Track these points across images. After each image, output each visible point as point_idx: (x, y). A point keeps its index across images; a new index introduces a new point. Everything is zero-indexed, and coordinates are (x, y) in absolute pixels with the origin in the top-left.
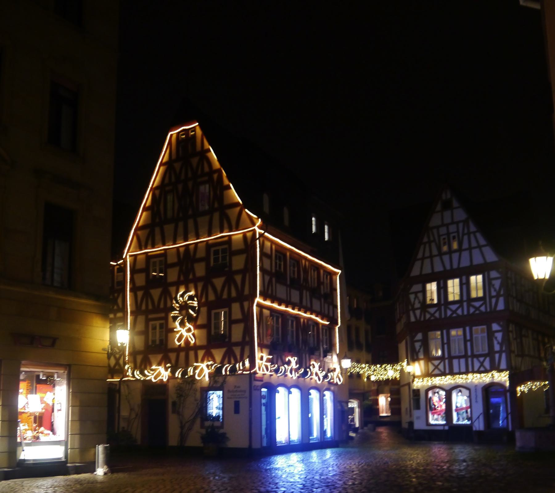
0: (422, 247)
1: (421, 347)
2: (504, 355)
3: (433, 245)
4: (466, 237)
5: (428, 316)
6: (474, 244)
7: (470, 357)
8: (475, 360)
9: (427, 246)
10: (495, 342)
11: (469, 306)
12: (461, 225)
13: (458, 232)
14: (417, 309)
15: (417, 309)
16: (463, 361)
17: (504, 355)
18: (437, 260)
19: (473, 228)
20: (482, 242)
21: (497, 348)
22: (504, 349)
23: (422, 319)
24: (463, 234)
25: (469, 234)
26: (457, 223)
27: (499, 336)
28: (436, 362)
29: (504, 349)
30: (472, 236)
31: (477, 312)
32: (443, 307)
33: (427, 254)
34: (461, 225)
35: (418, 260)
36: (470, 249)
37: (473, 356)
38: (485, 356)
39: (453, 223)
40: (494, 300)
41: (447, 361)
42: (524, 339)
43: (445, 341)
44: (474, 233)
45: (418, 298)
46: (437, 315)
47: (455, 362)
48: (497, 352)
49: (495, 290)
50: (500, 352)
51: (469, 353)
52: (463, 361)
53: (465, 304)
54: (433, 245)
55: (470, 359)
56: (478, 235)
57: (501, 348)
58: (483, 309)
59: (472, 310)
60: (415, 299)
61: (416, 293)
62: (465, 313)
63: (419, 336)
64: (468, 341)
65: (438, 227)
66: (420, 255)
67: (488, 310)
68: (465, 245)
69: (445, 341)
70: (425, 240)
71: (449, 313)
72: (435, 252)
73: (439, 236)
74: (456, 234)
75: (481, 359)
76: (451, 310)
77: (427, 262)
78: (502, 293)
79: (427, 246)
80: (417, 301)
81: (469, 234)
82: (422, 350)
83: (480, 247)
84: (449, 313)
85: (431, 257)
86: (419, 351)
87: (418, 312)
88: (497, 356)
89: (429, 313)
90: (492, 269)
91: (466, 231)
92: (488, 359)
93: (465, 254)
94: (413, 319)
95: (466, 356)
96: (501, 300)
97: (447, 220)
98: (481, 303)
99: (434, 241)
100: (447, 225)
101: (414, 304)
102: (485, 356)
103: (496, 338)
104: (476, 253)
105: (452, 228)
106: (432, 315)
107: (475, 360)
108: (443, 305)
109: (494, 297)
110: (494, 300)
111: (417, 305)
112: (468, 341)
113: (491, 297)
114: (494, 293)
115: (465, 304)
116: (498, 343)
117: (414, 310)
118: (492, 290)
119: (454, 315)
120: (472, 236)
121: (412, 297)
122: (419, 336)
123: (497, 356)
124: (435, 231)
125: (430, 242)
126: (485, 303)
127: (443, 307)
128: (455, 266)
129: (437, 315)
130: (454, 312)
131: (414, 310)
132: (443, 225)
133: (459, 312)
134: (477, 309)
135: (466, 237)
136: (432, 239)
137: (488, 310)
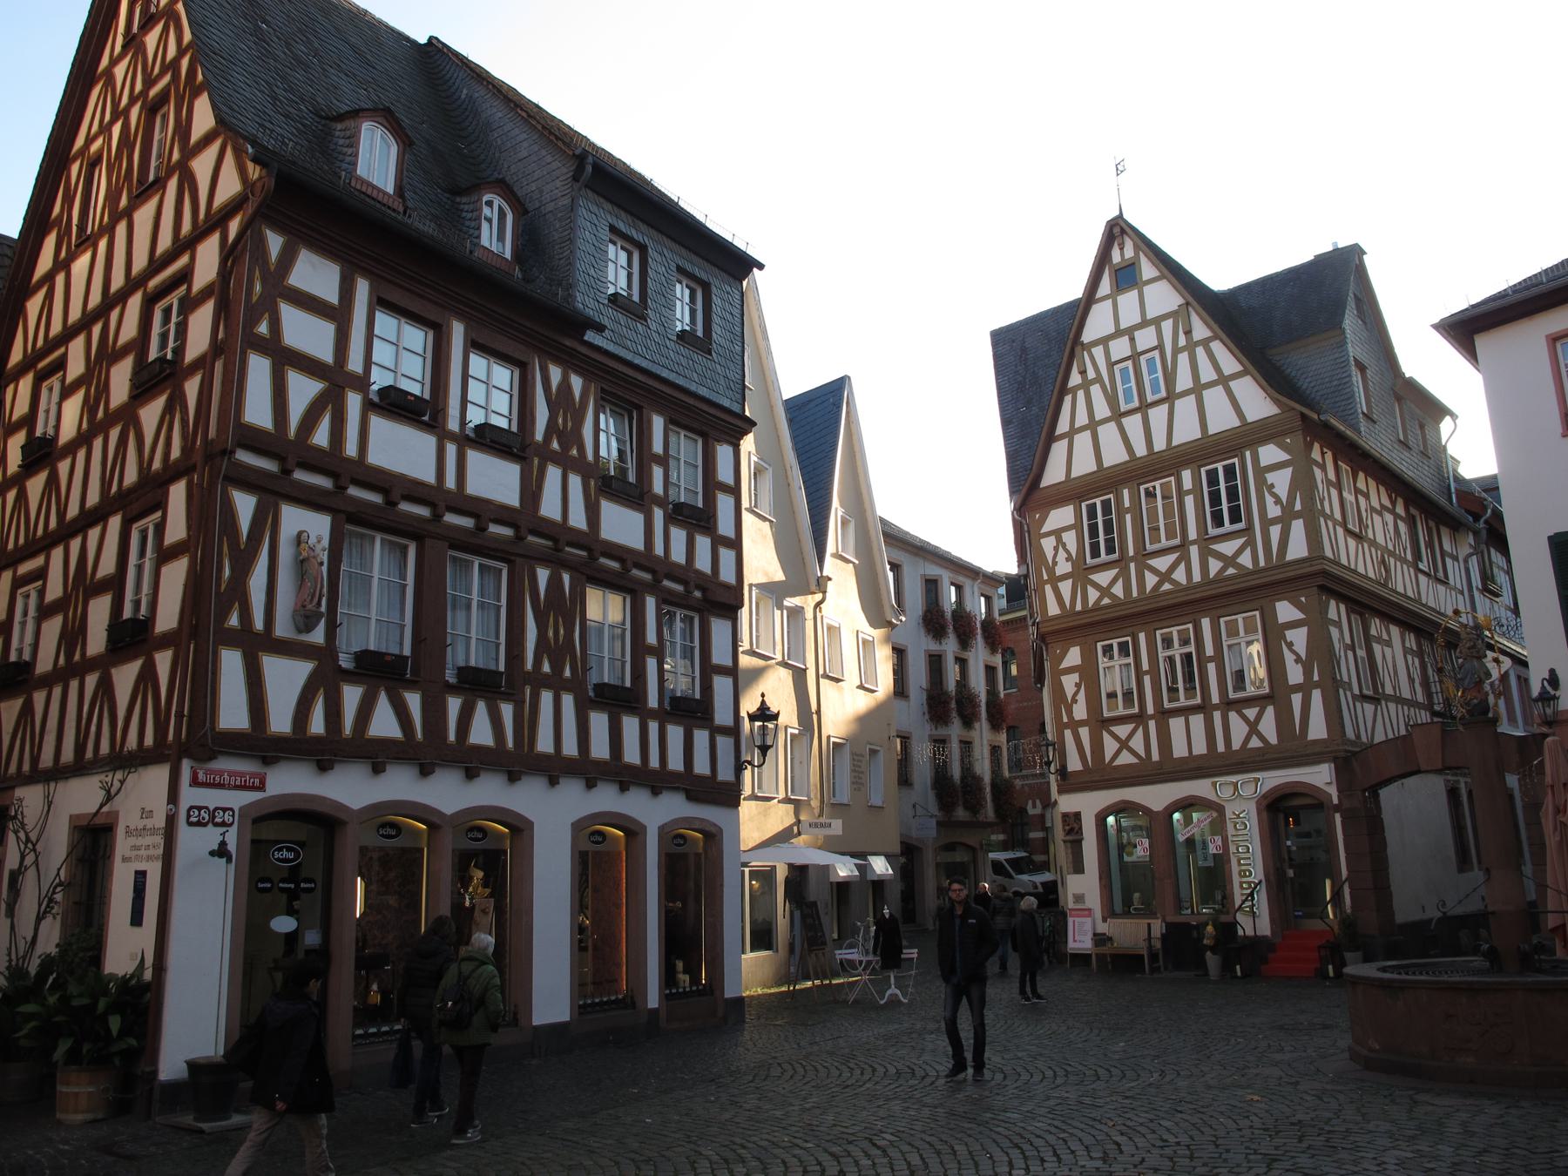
0: (1068, 399)
1: (1078, 686)
2: (1316, 695)
3: (1095, 390)
4: (1183, 358)
5: (1093, 595)
6: (1207, 374)
7: (1216, 707)
8: (1233, 715)
9: (1081, 394)
10: (1289, 658)
11: (1205, 555)
12: (1167, 326)
13: (1160, 347)
14: (1064, 577)
15: (1064, 577)
16: (1197, 721)
17: (1316, 695)
18: (1108, 433)
19: (1200, 331)
20: (1230, 364)
21: (1295, 675)
22: (1316, 678)
23: (1079, 607)
24: (1176, 351)
25: (1191, 347)
26: (1157, 322)
27: (1299, 638)
28: (1122, 731)
29: (1316, 678)
30: (1200, 351)
31: (1231, 571)
32: (1132, 565)
33: (1082, 419)
34: (1167, 326)
35: (1062, 437)
36: (1198, 389)
37: (1228, 705)
38: (1260, 701)
39: (1145, 323)
40: (1275, 531)
41: (1152, 724)
42: (1377, 648)
43: (1145, 666)
44: (1205, 343)
45: (1064, 545)
46: (1118, 590)
47: (1176, 724)
48: (1297, 688)
49: (1278, 501)
50: (1305, 689)
51: (1215, 699)
52: (1197, 721)
53: (1194, 551)
54: (1095, 390)
55: (1217, 715)
56: (1216, 346)
57: (1308, 673)
58: (1246, 560)
59: (1215, 566)
60: (1056, 549)
61: (1057, 533)
62: (1197, 577)
63: (1074, 656)
64: (1211, 659)
65: (1104, 341)
66: (1063, 426)
67: (1262, 563)
68: (1184, 381)
69: (1145, 666)
70: (1075, 379)
71: (1151, 580)
72: (1102, 410)
73: (1111, 365)
74: (1156, 354)
75: (1251, 713)
76: (1154, 571)
77: (1083, 441)
78: (1298, 506)
79: (1081, 394)
80: (1062, 555)
81: (1191, 347)
82: (1081, 697)
83: (1223, 380)
84: (1151, 580)
85: (1093, 425)
86: (1074, 701)
87: (1066, 587)
88: (1297, 699)
89: (1096, 586)
90: (1264, 441)
91: (1182, 341)
92: (1270, 710)
93: (1186, 408)
94: (1053, 609)
95: (1204, 708)
96: (1298, 527)
97: (1130, 317)
98: (1240, 542)
99: (1099, 379)
100: (1130, 332)
101: (1055, 563)
102: (1260, 701)
103: (1290, 645)
104: (1215, 399)
105: (1146, 338)
106: (1105, 591)
107: (1233, 715)
108: (1132, 559)
109: (1275, 521)
110: (1275, 531)
111: (1063, 567)
112: (1211, 659)
113: (1267, 523)
114: (1274, 511)
115: (1194, 551)
116: (1298, 660)
117: (1055, 580)
118: (1269, 500)
119: (1167, 586)
120: (1200, 351)
121: (1048, 544)
122: (1074, 656)
123: (1297, 699)
124: (1098, 352)
125: (1086, 385)
126: (1251, 543)
127: (1132, 565)
128: (1160, 444)
129: (1118, 590)
130: (1165, 577)
131: (1055, 580)
132: (1118, 333)
133: (1180, 575)
134: (1229, 561)
135: (1183, 358)
136: (1091, 374)
137: (1262, 563)
